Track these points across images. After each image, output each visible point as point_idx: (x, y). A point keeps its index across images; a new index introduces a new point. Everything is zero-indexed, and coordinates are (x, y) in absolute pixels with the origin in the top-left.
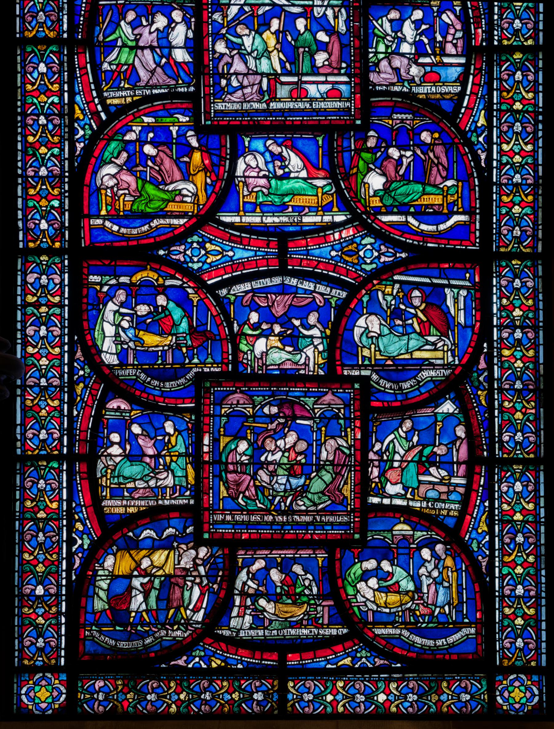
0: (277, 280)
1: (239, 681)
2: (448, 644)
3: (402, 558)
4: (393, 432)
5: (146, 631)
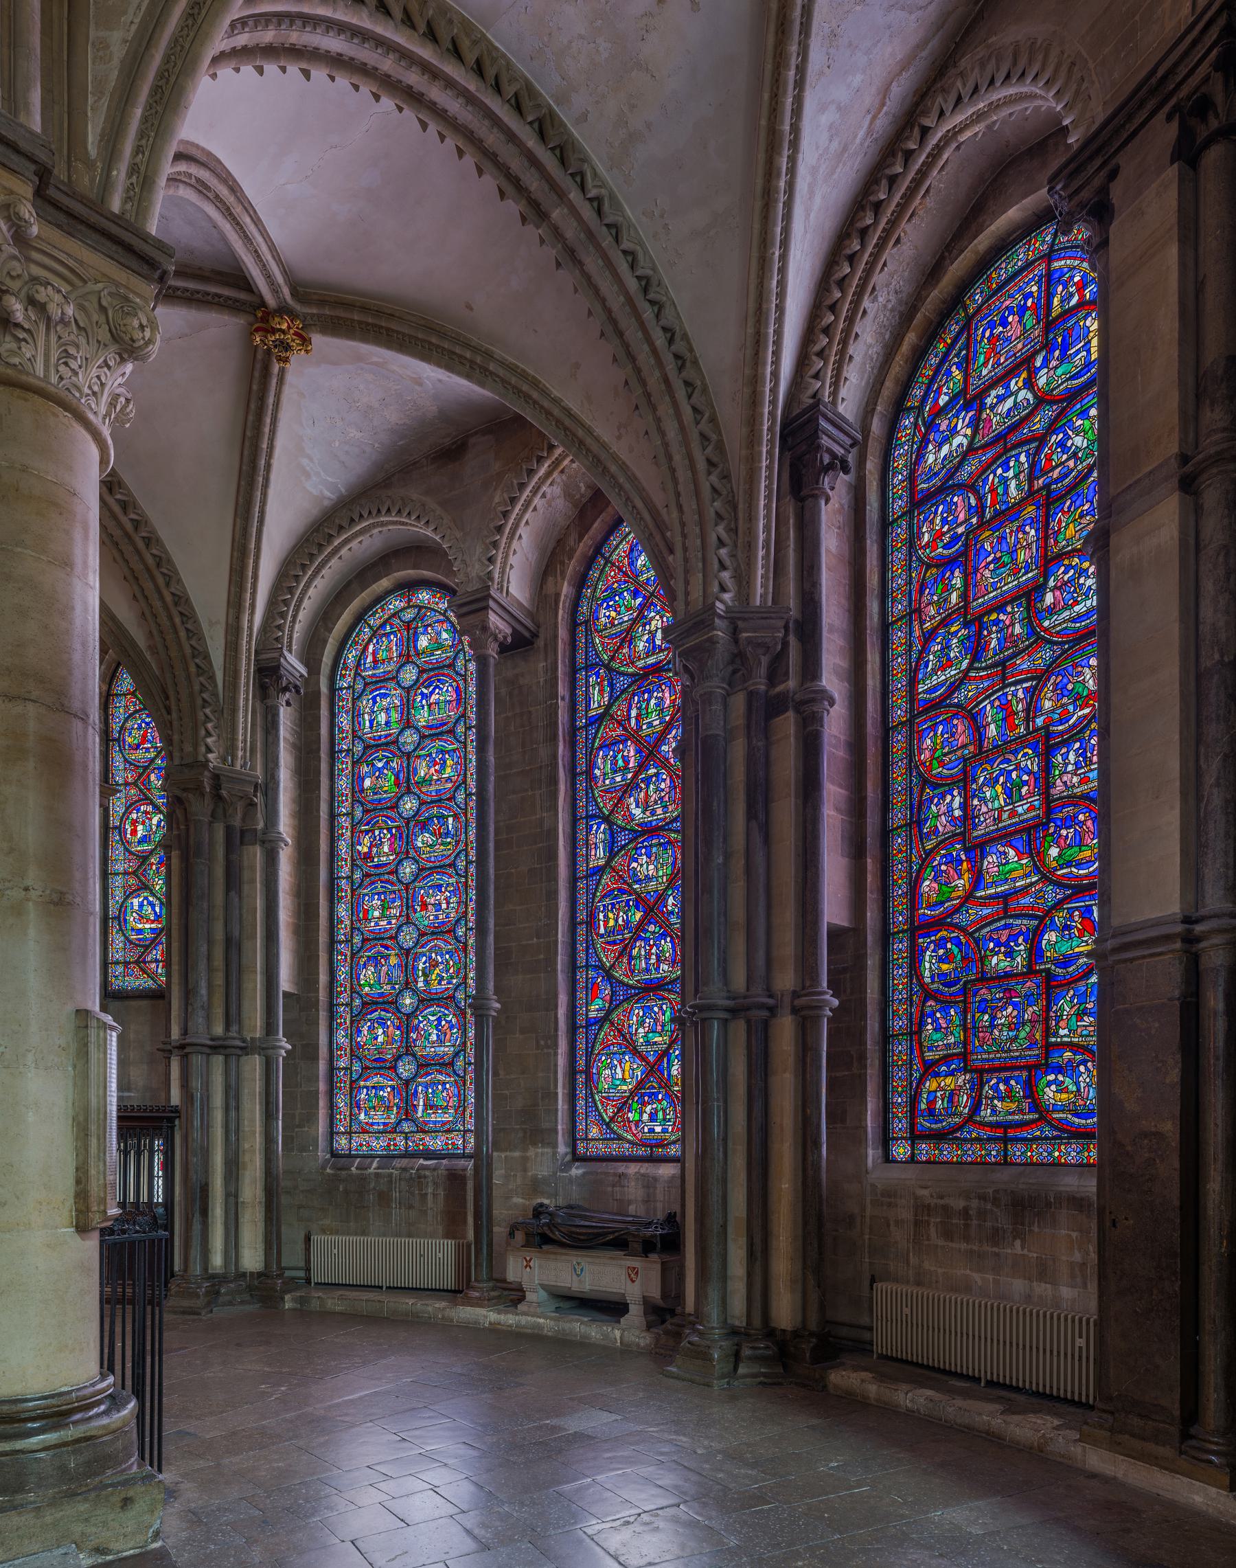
0: (1003, 922)
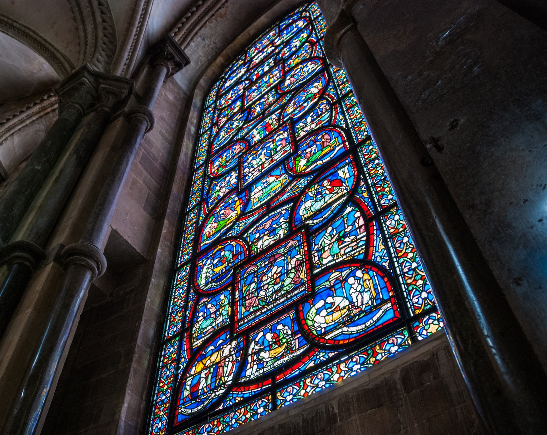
1: (250, 405)
2: (374, 322)
3: (338, 291)
4: (323, 237)
5: (205, 398)
